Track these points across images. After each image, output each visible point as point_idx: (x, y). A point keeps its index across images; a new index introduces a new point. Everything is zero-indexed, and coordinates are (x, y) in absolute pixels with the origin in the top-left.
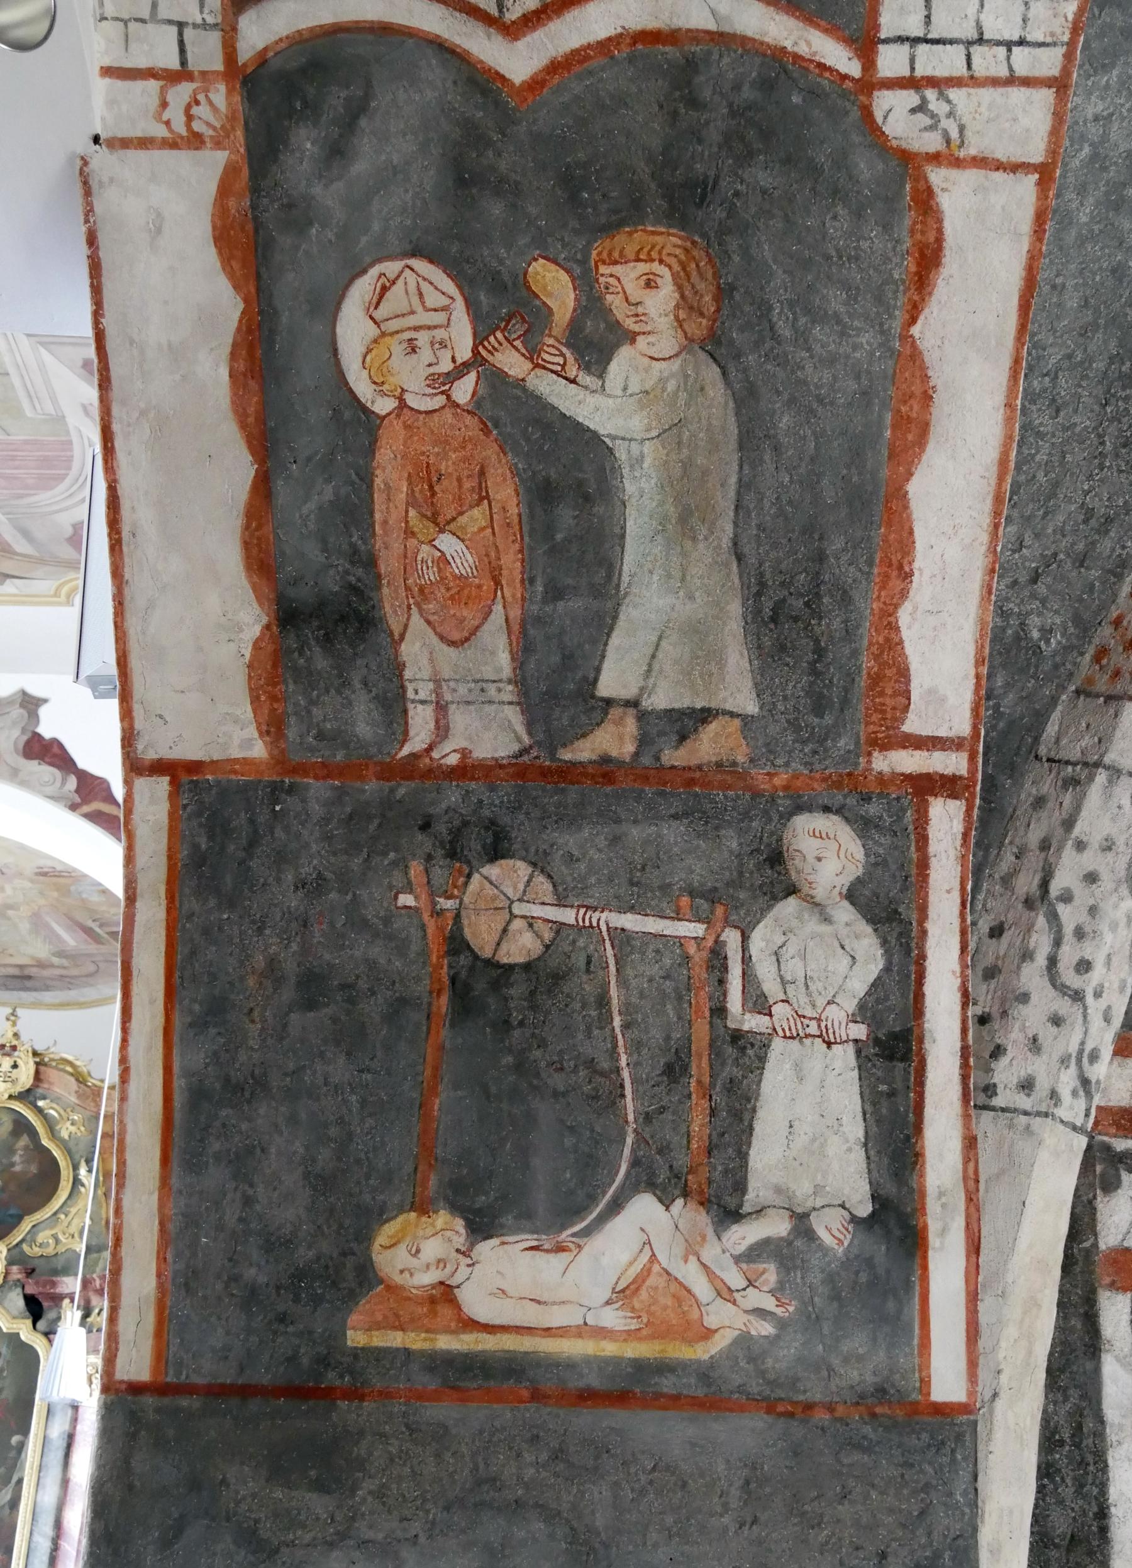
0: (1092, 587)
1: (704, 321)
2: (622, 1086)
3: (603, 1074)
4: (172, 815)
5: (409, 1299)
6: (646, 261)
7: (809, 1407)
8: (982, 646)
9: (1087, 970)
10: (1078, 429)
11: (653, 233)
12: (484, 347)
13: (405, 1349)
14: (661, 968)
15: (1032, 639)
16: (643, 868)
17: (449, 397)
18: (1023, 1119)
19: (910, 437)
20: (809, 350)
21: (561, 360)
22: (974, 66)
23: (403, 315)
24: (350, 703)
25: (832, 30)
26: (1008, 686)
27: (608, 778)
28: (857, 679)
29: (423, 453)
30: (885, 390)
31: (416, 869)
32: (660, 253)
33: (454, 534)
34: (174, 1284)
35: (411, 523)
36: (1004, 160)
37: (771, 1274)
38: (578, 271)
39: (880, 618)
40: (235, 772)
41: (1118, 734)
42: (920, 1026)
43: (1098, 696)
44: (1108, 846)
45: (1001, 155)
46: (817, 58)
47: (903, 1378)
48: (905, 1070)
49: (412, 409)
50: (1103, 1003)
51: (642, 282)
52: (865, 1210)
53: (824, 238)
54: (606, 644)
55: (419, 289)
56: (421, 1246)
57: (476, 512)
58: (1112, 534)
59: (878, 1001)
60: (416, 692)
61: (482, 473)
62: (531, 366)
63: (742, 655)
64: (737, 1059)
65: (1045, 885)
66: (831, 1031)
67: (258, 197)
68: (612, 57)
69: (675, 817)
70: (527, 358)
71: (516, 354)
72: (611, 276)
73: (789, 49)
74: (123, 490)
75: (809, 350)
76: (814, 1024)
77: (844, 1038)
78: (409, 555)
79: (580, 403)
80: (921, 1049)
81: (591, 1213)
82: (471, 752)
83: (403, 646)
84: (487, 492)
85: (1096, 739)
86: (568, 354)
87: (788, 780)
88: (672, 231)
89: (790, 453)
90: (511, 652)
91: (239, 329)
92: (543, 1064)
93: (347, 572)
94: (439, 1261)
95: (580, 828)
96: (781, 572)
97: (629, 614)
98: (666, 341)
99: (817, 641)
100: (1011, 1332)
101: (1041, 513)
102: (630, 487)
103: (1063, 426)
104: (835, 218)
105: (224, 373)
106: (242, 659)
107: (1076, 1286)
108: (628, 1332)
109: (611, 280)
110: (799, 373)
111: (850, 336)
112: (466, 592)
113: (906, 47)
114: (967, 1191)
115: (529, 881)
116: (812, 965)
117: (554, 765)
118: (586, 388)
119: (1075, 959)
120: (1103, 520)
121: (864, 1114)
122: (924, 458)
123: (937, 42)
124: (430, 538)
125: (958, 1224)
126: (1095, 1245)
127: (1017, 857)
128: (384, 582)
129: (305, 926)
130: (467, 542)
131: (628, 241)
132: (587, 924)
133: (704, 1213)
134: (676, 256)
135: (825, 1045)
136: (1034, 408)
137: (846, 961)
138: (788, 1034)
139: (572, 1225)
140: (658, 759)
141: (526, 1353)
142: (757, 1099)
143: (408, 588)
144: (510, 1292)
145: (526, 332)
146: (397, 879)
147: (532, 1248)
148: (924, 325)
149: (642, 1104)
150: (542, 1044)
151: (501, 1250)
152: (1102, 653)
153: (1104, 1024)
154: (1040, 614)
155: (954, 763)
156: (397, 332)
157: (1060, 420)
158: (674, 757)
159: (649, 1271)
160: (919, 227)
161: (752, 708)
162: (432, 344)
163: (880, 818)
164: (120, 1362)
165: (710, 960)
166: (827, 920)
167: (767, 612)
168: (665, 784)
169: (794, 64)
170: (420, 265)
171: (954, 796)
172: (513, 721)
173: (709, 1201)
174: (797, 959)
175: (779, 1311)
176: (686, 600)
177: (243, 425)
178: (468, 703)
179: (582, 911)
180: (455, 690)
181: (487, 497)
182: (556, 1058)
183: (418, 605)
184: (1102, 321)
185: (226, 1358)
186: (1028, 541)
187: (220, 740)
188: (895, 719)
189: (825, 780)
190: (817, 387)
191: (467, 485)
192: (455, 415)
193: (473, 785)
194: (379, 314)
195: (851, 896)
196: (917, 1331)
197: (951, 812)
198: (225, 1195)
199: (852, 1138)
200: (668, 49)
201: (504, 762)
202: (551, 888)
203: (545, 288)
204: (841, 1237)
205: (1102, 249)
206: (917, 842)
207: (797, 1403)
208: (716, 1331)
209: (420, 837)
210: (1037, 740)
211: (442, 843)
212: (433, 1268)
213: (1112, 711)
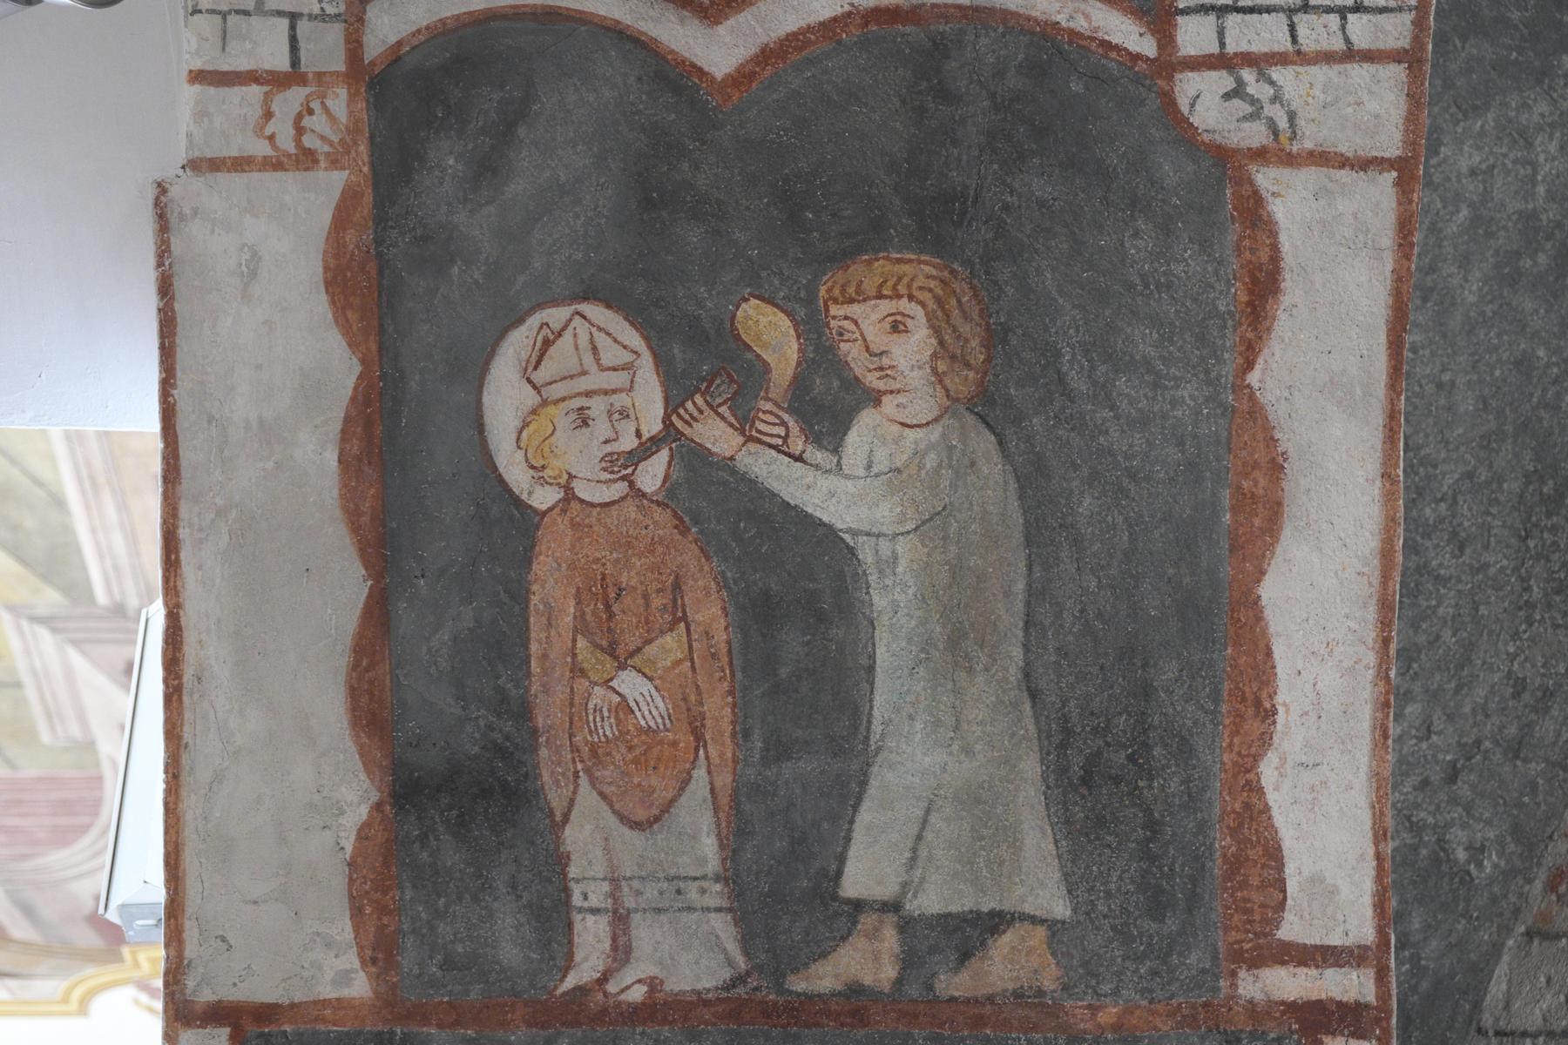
0: (1534, 787)
1: (971, 375)
6: (890, 298)
8: (1382, 813)
10: (1492, 571)
11: (899, 261)
12: (679, 416)
15: (1456, 861)
17: (632, 484)
19: (1257, 522)
21: (781, 431)
22: (1301, 40)
23: (572, 377)
27: (859, 1016)
28: (1209, 864)
29: (597, 561)
30: (1218, 459)
32: (909, 286)
33: (639, 671)
35: (580, 657)
36: (1350, 155)
38: (802, 313)
39: (1235, 776)
45: (1345, 148)
46: (1100, 35)
49: (582, 501)
53: (1123, 261)
54: (852, 822)
55: (592, 341)
57: (669, 640)
58: (1555, 713)
60: (586, 897)
61: (677, 586)
62: (741, 439)
67: (384, 229)
68: (839, 42)
70: (736, 429)
71: (722, 425)
72: (846, 318)
73: (1064, 24)
74: (189, 618)
75: (1112, 408)
78: (577, 700)
79: (808, 487)
82: (662, 982)
83: (568, 831)
84: (684, 612)
86: (791, 424)
88: (923, 258)
90: (719, 835)
91: (353, 399)
93: (490, 728)
96: (1092, 713)
97: (883, 778)
98: (923, 405)
99: (1148, 811)
101: (1453, 685)
102: (879, 601)
103: (1471, 567)
104: (1136, 235)
105: (331, 457)
106: (340, 855)
109: (847, 324)
110: (1102, 439)
111: (1166, 388)
112: (656, 751)
113: (1212, 18)
117: (781, 1000)
118: (817, 467)
120: (1539, 694)
122: (1279, 550)
124: (606, 676)
128: (542, 740)
130: (658, 682)
131: (871, 271)
134: (930, 290)
136: (1428, 543)
140: (930, 988)
143: (575, 749)
145: (735, 393)
148: (1264, 371)
154: (1464, 826)
156: (563, 399)
157: (1466, 558)
158: (954, 984)
160: (1247, 243)
161: (1061, 909)
162: (610, 414)
167: (1076, 771)
168: (941, 1026)
169: (1070, 43)
170: (594, 311)
172: (722, 935)
176: (962, 757)
177: (355, 528)
178: (659, 911)
181: (684, 618)
183: (588, 771)
184: (1509, 428)
186: (1438, 724)
187: (305, 974)
189: (1171, 1014)
190: (1127, 457)
191: (657, 602)
200: (908, 29)
201: (710, 996)
203: (758, 337)
205: (1499, 335)
210: (1477, 1006)
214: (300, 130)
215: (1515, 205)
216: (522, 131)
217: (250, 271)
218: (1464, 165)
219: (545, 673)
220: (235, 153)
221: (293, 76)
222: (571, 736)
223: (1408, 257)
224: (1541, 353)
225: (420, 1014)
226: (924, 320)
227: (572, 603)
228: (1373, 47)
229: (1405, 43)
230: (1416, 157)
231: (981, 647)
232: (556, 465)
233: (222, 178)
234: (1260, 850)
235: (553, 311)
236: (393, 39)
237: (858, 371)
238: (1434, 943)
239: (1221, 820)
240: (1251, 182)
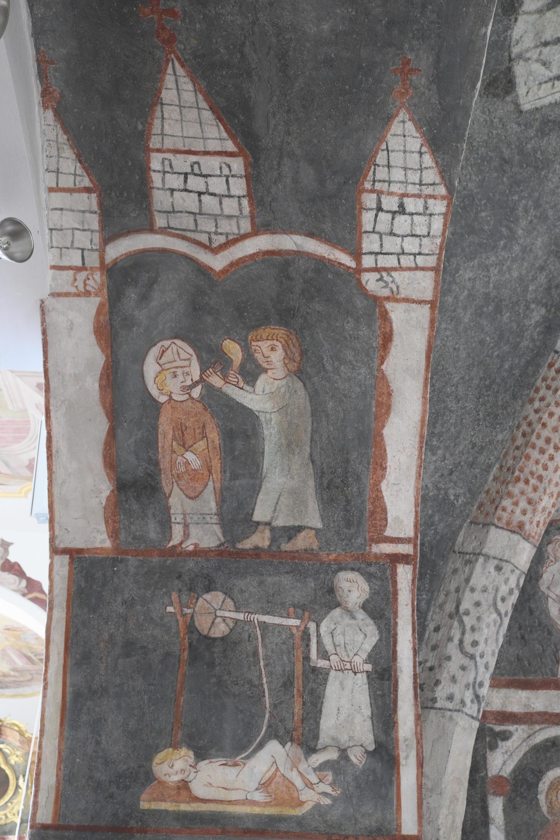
0: (476, 477)
1: (296, 364)
2: (264, 692)
3: (255, 686)
4: (70, 572)
5: (168, 787)
8: (418, 499)
9: (476, 646)
10: (468, 409)
11: (274, 329)
13: (166, 810)
14: (281, 639)
15: (450, 499)
16: (273, 595)
17: (190, 395)
18: (449, 713)
19: (383, 411)
20: (339, 375)
22: (401, 263)
23: (171, 362)
24: (147, 523)
26: (440, 520)
27: (258, 556)
28: (365, 513)
29: (179, 418)
30: (372, 391)
31: (174, 596)
32: (277, 336)
34: (64, 780)
35: (174, 448)
36: (416, 299)
37: (330, 777)
38: (243, 344)
39: (374, 487)
40: (98, 554)
41: (488, 540)
42: (395, 665)
43: (479, 524)
44: (485, 590)
45: (414, 297)
47: (389, 824)
48: (389, 684)
49: (174, 400)
50: (484, 660)
52: (371, 748)
53: (344, 331)
54: (256, 498)
56: (174, 763)
57: (201, 443)
58: (484, 454)
59: (376, 654)
60: (176, 519)
61: (204, 426)
62: (224, 382)
63: (315, 503)
64: (314, 680)
65: (457, 607)
66: (356, 667)
68: (256, 261)
69: (287, 573)
71: (218, 378)
72: (257, 346)
73: (327, 257)
74: (54, 434)
75: (339, 375)
76: (348, 664)
77: (362, 670)
78: (173, 461)
80: (396, 675)
81: (250, 748)
85: (479, 543)
86: (240, 378)
87: (336, 557)
89: (333, 418)
90: (216, 502)
91: (103, 368)
92: (229, 682)
93: (146, 468)
94: (182, 770)
95: (246, 578)
97: (267, 486)
98: (280, 372)
99: (347, 497)
100: (444, 811)
101: (453, 444)
102: (266, 432)
103: (461, 407)
104: (348, 322)
105: (97, 386)
107: (477, 794)
108: (266, 803)
109: (257, 348)
110: (336, 385)
112: (197, 476)
113: (373, 256)
114: (417, 739)
115: (223, 601)
116: (347, 638)
117: (234, 551)
118: (247, 391)
119: (472, 640)
120: (480, 448)
121: (371, 704)
122: (389, 419)
125: (414, 753)
126: (486, 775)
127: (446, 596)
128: (162, 472)
129: (126, 620)
130: (198, 455)
131: (264, 332)
132: (249, 620)
133: (300, 749)
135: (353, 674)
136: (448, 400)
137: (362, 636)
138: (337, 669)
139: (241, 754)
140: (279, 548)
141: (220, 812)
142: (323, 698)
143: (172, 475)
144: (214, 785)
146: (166, 600)
148: (387, 365)
149: (273, 700)
150: (229, 673)
151: (209, 766)
152: (481, 505)
153: (485, 670)
155: (406, 549)
156: (169, 369)
157: (460, 405)
158: (286, 547)
159: (276, 775)
160: (383, 326)
161: (319, 525)
162: (183, 374)
163: (376, 573)
164: (39, 815)
165: (302, 636)
166: (353, 618)
167: (325, 484)
168: (282, 559)
169: (329, 263)
170: (178, 342)
171: (408, 563)
172: (217, 531)
173: (302, 743)
174: (341, 636)
175: (333, 793)
177: (104, 407)
178: (198, 524)
179: (247, 614)
181: (206, 436)
182: (235, 679)
183: (176, 482)
184: (476, 363)
185: (86, 814)
186: (448, 455)
188: (381, 530)
189: (352, 556)
190: (343, 390)
191: (198, 431)
192: (192, 403)
193: (200, 559)
194: (161, 362)
195: (364, 607)
196: (395, 803)
197: (407, 570)
199: (365, 714)
200: (278, 257)
202: (233, 604)
203: (229, 351)
204: (361, 760)
205: (475, 333)
206: (392, 584)
207: (341, 835)
208: (305, 802)
209: (176, 582)
210: (454, 544)
211: (186, 584)
212: (179, 773)
213: (485, 530)
215: (482, 290)
218: (467, 277)
219: (163, 452)
222: (171, 471)
223: (433, 331)
224: (488, 339)
225: (126, 552)
226: (281, 347)
227: (172, 431)
228: (424, 266)
229: (434, 265)
230: (436, 300)
231: (297, 447)
232: (167, 389)
234: (380, 509)
235: (165, 342)
237: (261, 362)
238: (442, 525)
239: (369, 500)
240: (384, 307)
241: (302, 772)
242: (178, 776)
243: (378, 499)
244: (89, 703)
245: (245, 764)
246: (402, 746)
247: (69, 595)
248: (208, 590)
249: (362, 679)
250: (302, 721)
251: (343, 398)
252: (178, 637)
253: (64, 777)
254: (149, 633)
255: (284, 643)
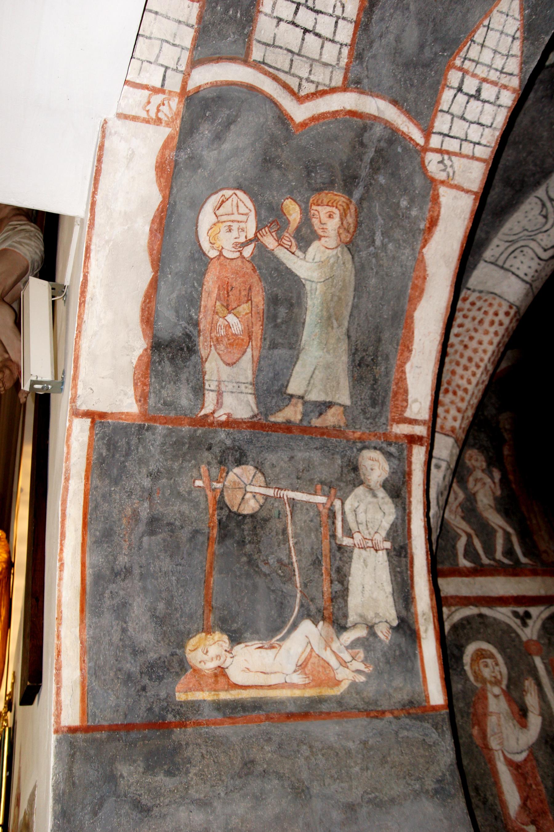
2: (294, 571)
3: (285, 565)
4: (90, 438)
5: (204, 675)
7: (383, 712)
11: (336, 195)
17: (241, 253)
20: (386, 252)
21: (290, 244)
24: (180, 388)
25: (417, 125)
29: (226, 277)
30: (411, 273)
31: (204, 468)
32: (337, 204)
37: (362, 655)
38: (303, 206)
40: (122, 419)
42: (410, 543)
46: (410, 135)
51: (327, 215)
52: (395, 623)
54: (293, 370)
55: (237, 204)
57: (245, 306)
61: (250, 289)
62: (276, 244)
71: (272, 239)
75: (386, 252)
76: (370, 542)
78: (214, 322)
91: (158, 210)
94: (217, 656)
95: (277, 452)
99: (375, 376)
102: (310, 302)
105: (147, 229)
108: (305, 685)
112: (236, 341)
115: (254, 476)
118: (298, 257)
123: (452, 137)
131: (325, 196)
139: (277, 635)
141: (261, 698)
143: (211, 338)
144: (251, 670)
146: (195, 473)
147: (259, 648)
150: (259, 551)
158: (316, 422)
159: (311, 655)
162: (238, 229)
164: (63, 716)
166: (375, 496)
170: (240, 193)
174: (363, 514)
175: (366, 670)
177: (151, 254)
178: (232, 392)
180: (226, 386)
181: (251, 300)
182: (265, 558)
183: (215, 345)
185: (117, 711)
187: (117, 403)
192: (243, 262)
193: (232, 430)
194: (218, 213)
195: (384, 486)
196: (421, 675)
198: (112, 628)
202: (263, 479)
203: (289, 212)
208: (342, 681)
209: (206, 454)
211: (216, 457)
212: (214, 659)
214: (158, 110)
216: (232, 127)
217: (131, 157)
219: (205, 312)
220: (134, 114)
221: (161, 90)
222: (211, 333)
225: (154, 419)
227: (217, 290)
232: (218, 244)
233: (127, 122)
236: (198, 85)
237: (316, 228)
241: (336, 651)
242: (213, 662)
243: (402, 379)
244: (112, 586)
245: (280, 646)
246: (421, 620)
247: (88, 464)
248: (239, 462)
249: (382, 556)
250: (332, 600)
251: (385, 276)
252: (206, 513)
253: (89, 670)
254: (176, 508)
255: (311, 521)
